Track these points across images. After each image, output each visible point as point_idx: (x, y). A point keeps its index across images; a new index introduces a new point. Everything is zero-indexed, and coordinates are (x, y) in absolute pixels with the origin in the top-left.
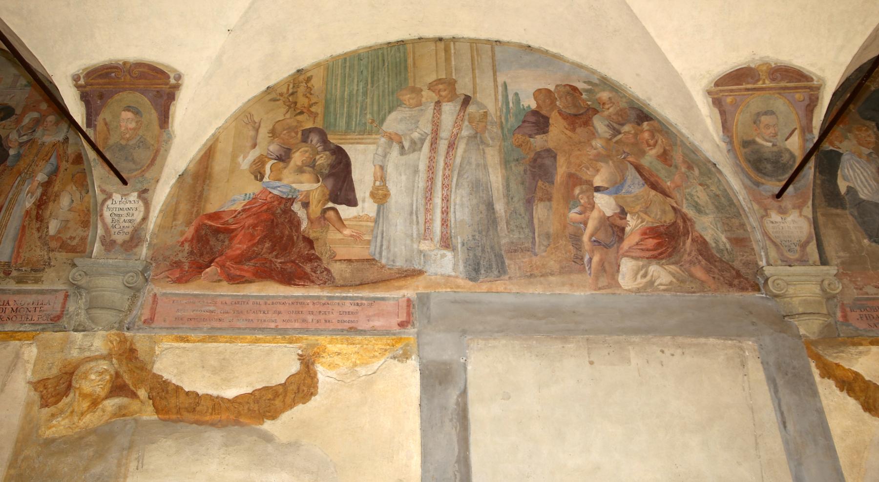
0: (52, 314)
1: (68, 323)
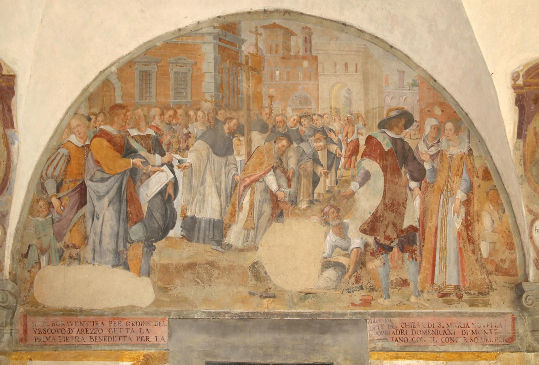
0: (506, 336)
1: (521, 344)
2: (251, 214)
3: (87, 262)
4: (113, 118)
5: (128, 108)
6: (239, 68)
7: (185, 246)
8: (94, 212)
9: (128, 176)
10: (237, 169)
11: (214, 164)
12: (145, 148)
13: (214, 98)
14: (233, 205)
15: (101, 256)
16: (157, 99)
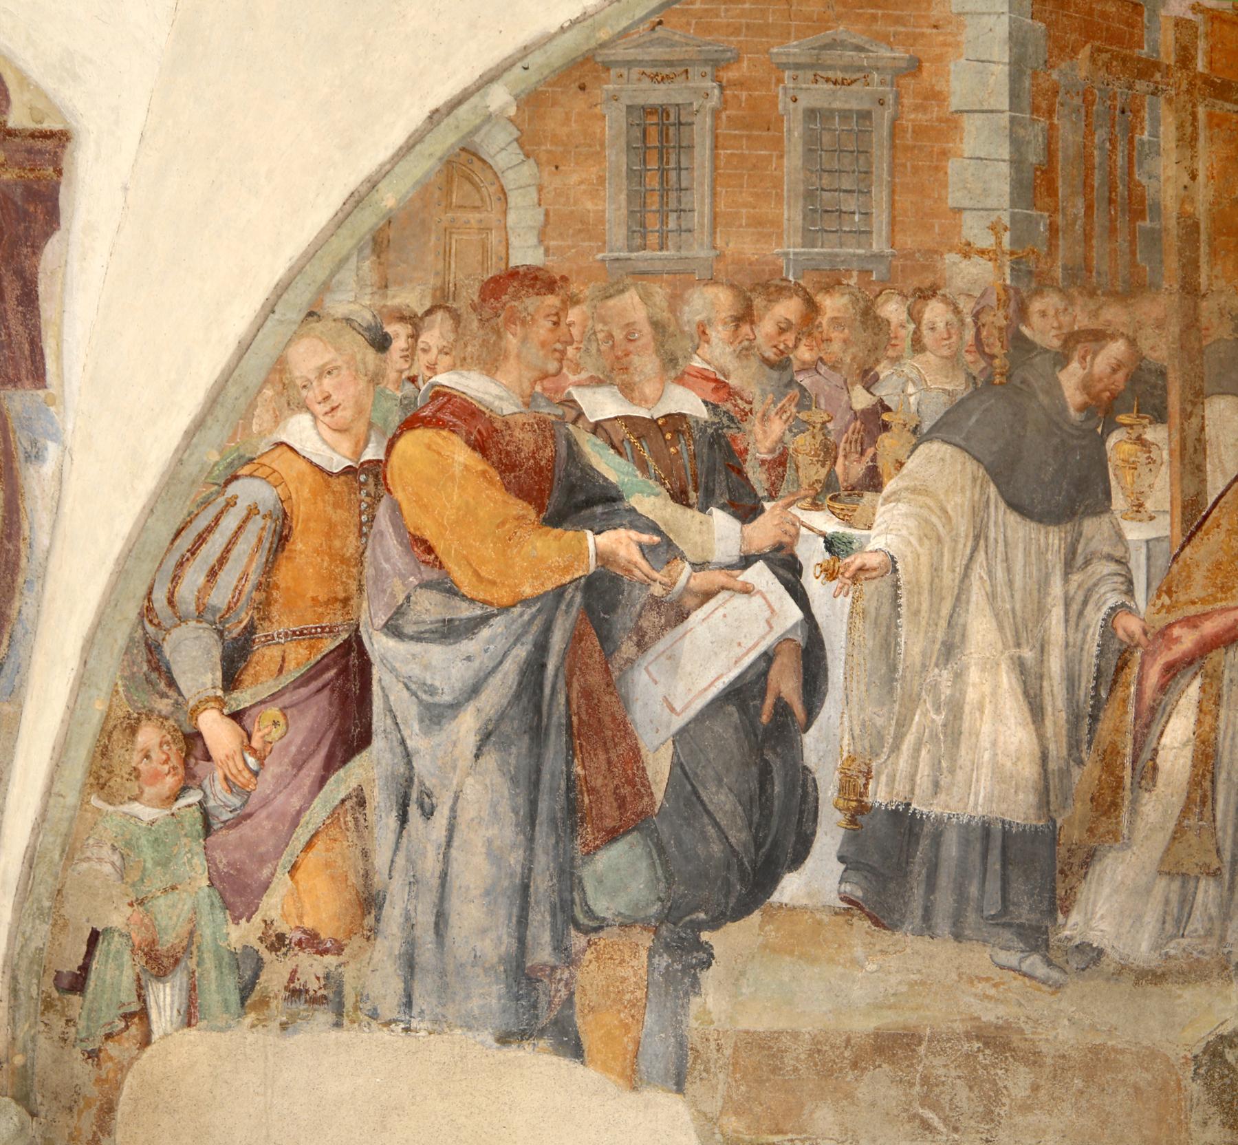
2: (1203, 803)
3: (374, 1015)
4: (499, 336)
5: (574, 288)
6: (1141, 86)
7: (859, 952)
8: (410, 781)
9: (574, 611)
10: (1131, 582)
11: (1006, 559)
12: (658, 478)
13: (1006, 238)
14: (1109, 758)
15: (444, 991)
16: (719, 242)
